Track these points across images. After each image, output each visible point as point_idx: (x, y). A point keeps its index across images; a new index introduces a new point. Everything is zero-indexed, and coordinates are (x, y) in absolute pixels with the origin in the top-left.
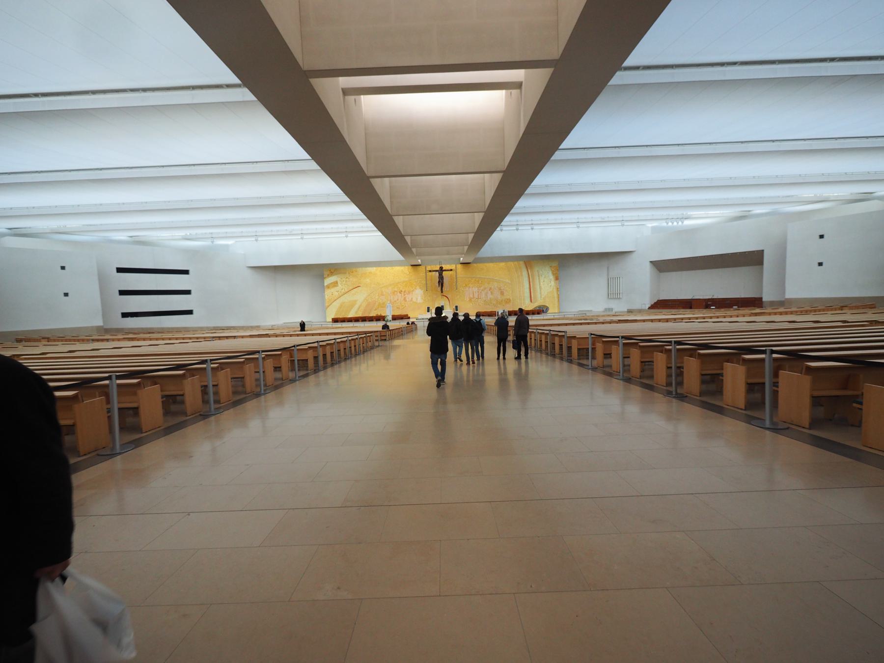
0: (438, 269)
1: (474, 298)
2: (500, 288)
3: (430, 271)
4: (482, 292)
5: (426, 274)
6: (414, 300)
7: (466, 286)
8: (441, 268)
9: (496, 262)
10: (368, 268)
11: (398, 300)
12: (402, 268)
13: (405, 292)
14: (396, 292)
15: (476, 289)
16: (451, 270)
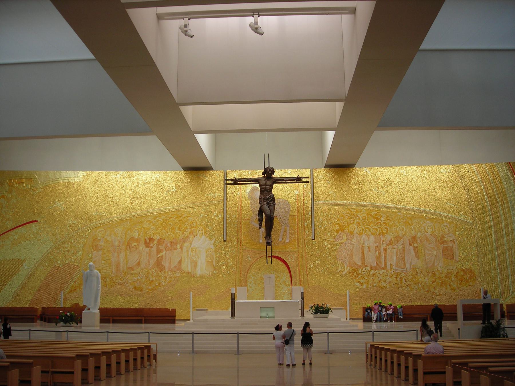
0: (259, 174)
1: (364, 264)
2: (442, 237)
3: (235, 181)
4: (390, 247)
5: (225, 190)
6: (186, 266)
7: (342, 229)
8: (269, 172)
9: (428, 164)
10: (64, 174)
11: (139, 264)
12: (159, 175)
13: (160, 241)
14: (137, 241)
15: (372, 239)
16: (298, 180)
